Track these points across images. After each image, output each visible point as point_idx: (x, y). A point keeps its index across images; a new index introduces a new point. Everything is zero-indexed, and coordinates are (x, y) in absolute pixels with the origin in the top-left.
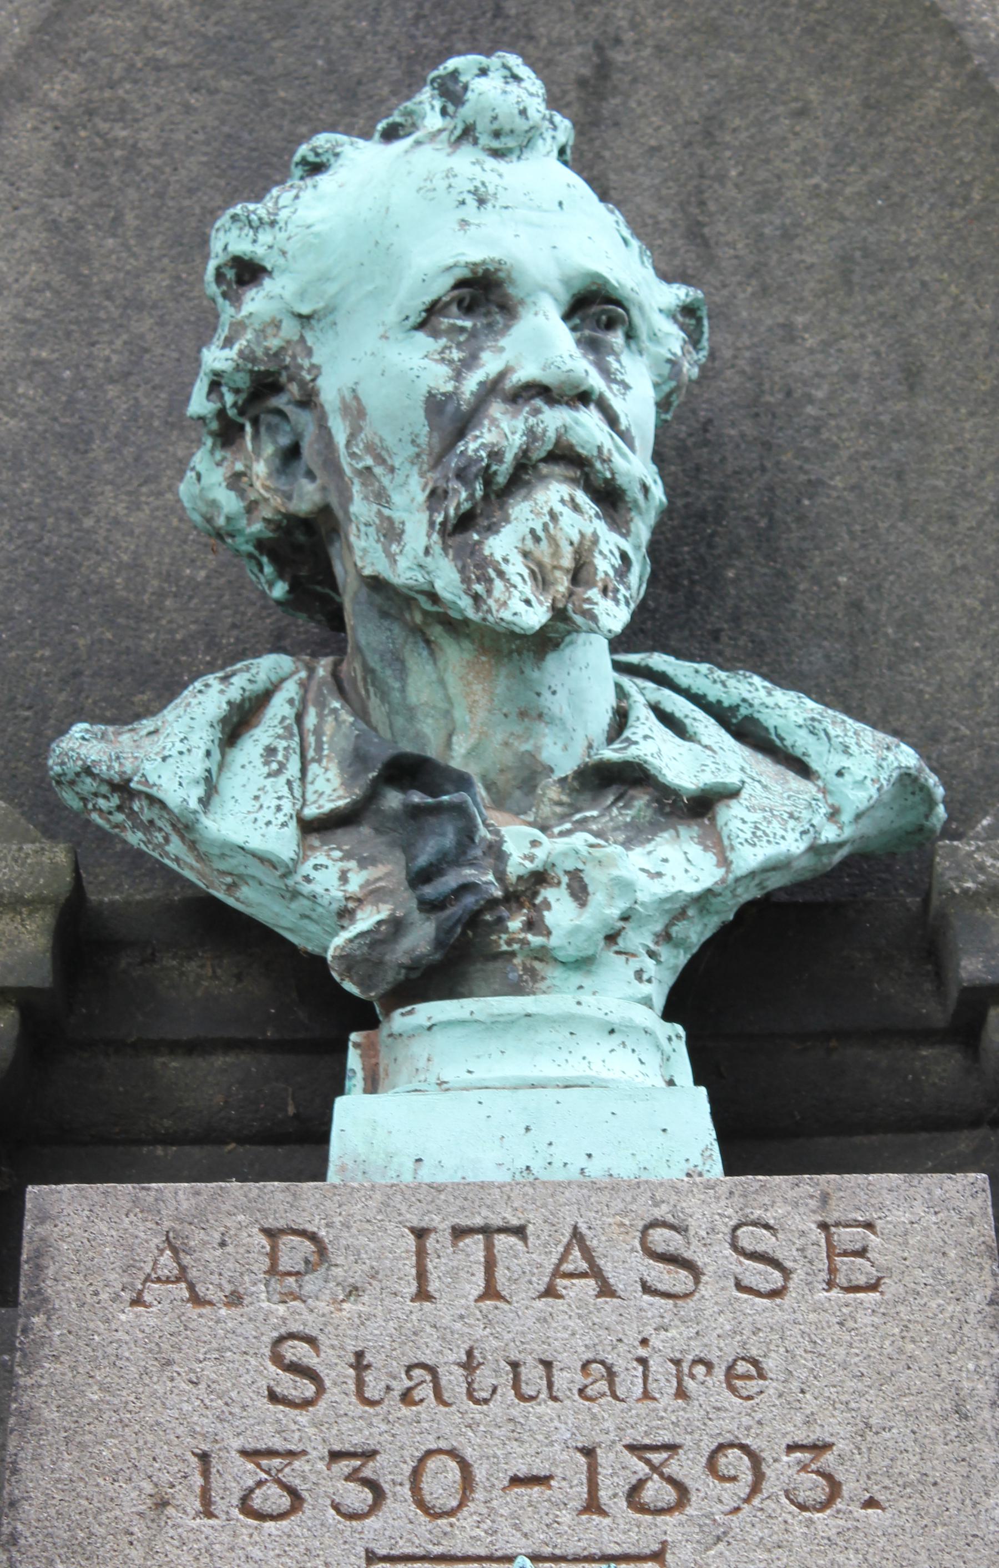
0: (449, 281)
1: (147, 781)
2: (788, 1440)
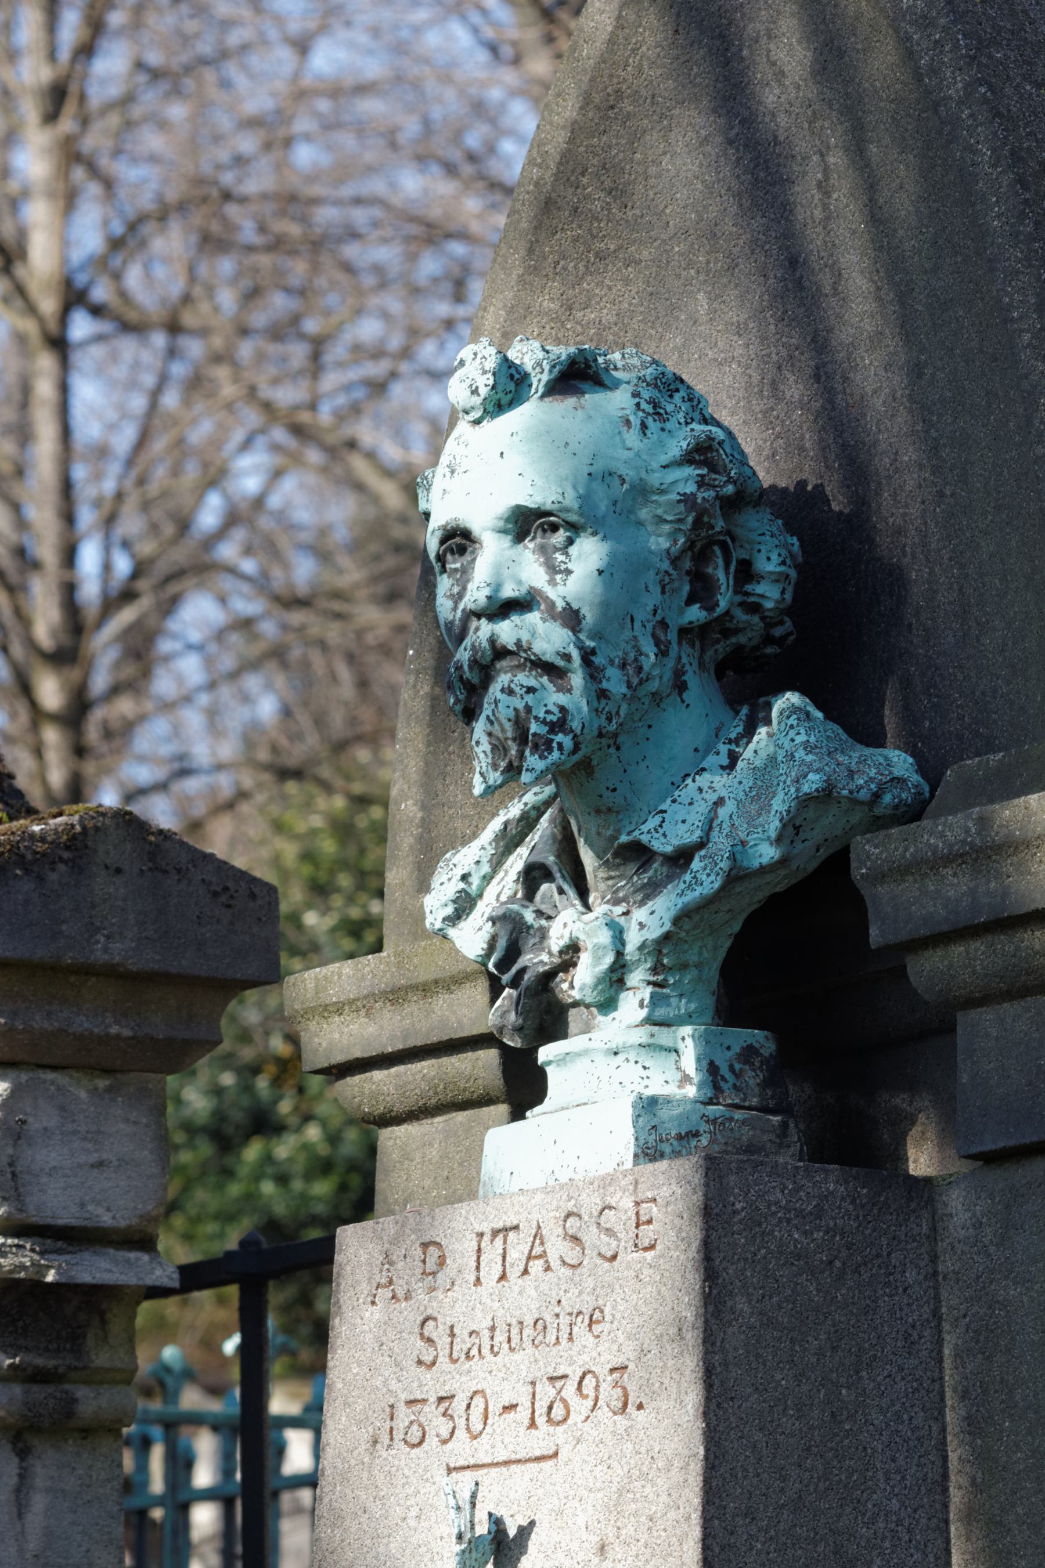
2: (609, 1366)
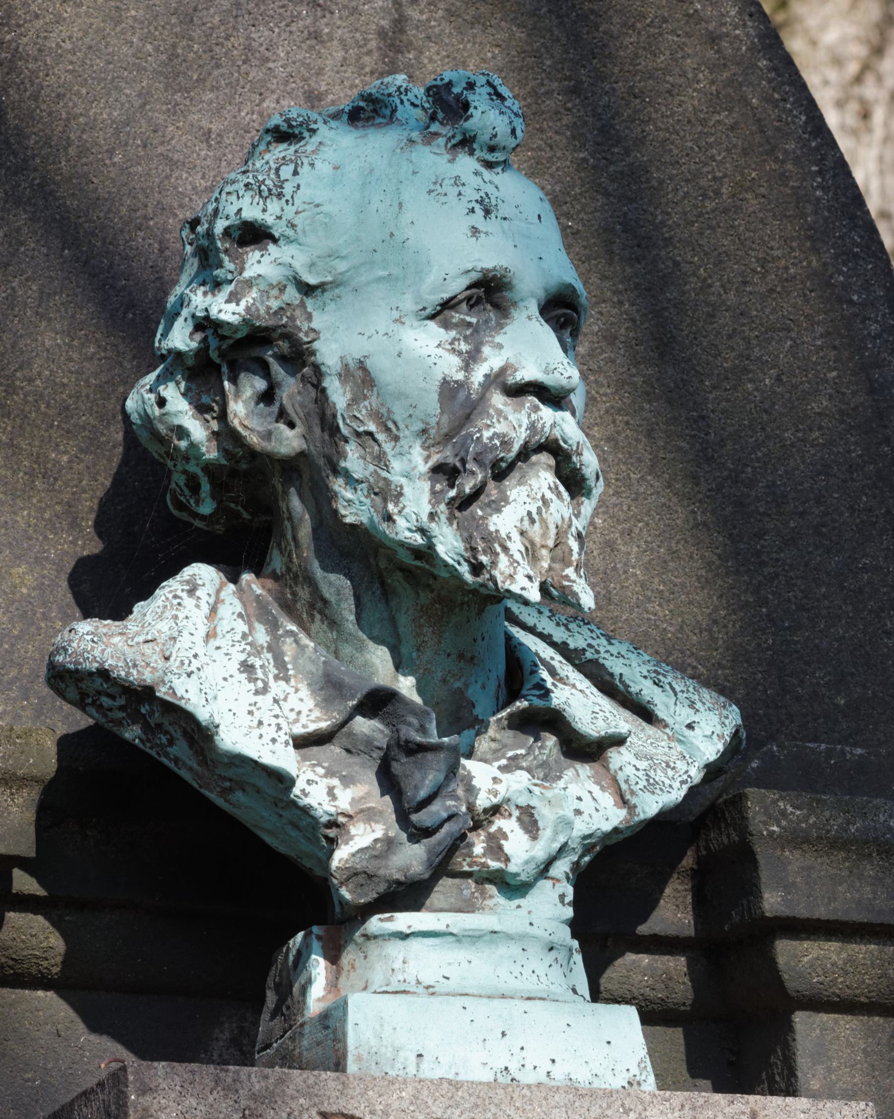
0: (465, 282)
1: (174, 692)
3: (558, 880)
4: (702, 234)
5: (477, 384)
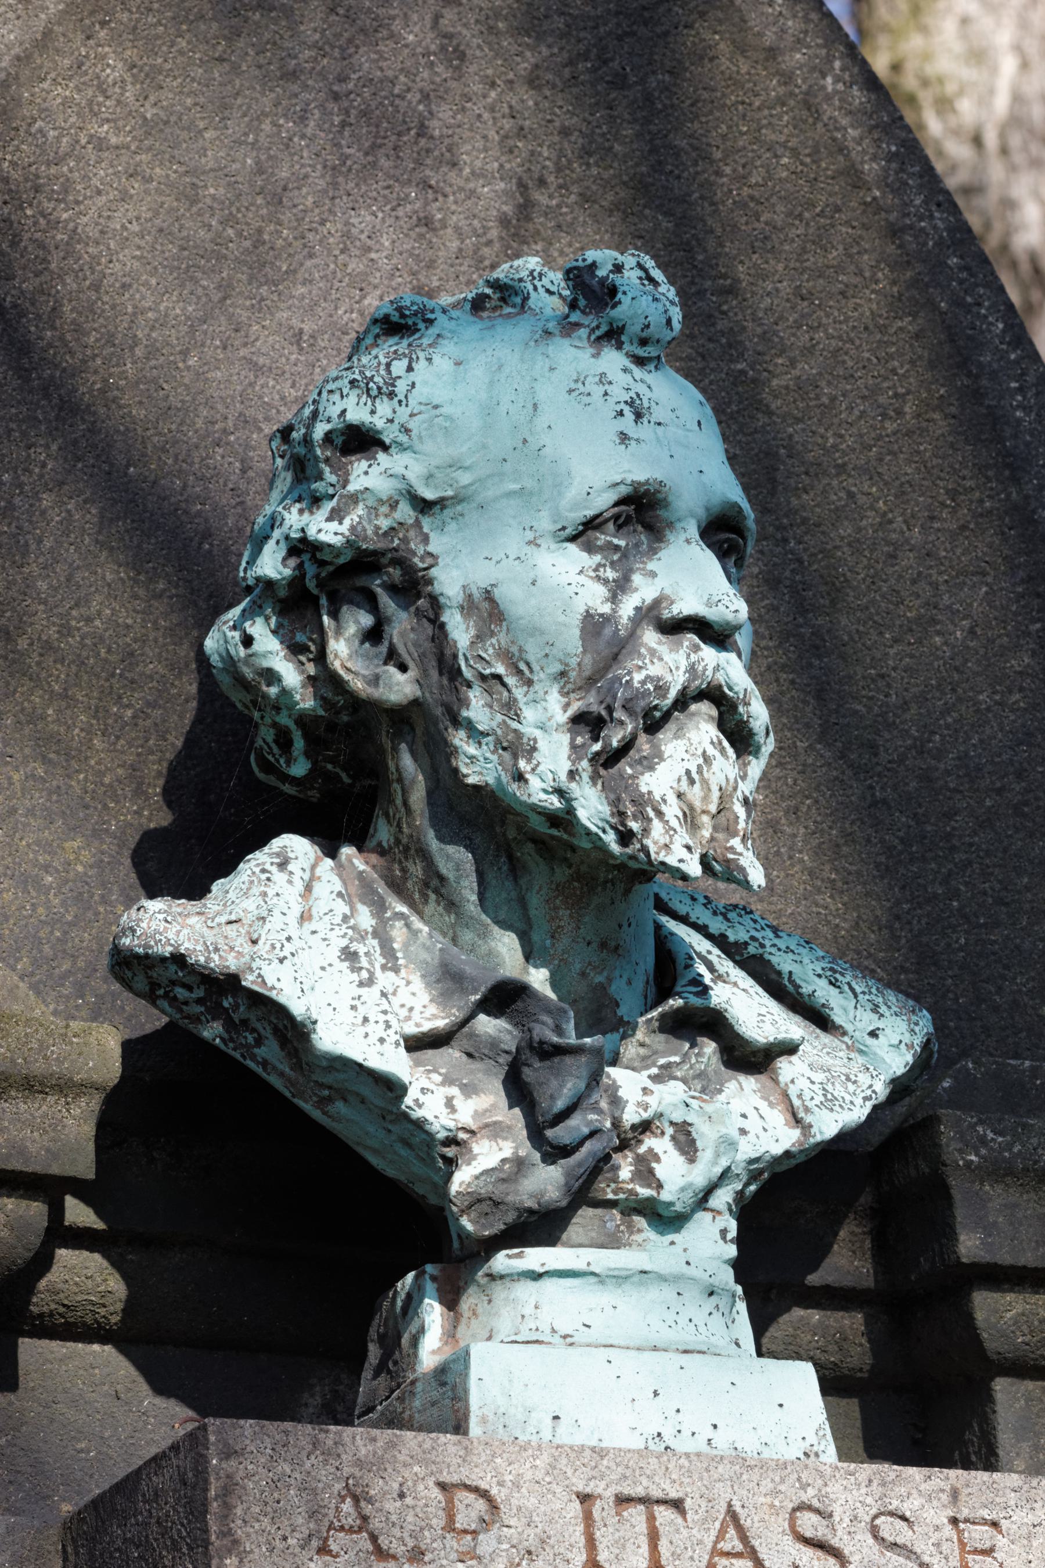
0: (612, 497)
1: (264, 981)
3: (719, 1213)
4: (881, 460)
5: (625, 618)
